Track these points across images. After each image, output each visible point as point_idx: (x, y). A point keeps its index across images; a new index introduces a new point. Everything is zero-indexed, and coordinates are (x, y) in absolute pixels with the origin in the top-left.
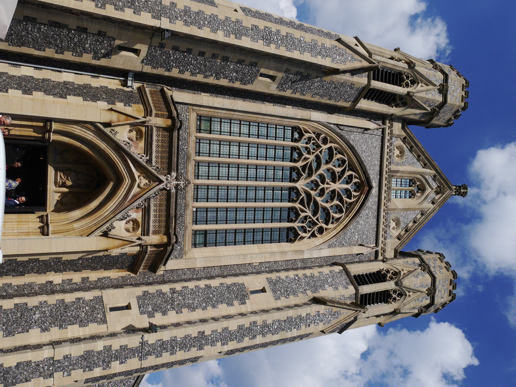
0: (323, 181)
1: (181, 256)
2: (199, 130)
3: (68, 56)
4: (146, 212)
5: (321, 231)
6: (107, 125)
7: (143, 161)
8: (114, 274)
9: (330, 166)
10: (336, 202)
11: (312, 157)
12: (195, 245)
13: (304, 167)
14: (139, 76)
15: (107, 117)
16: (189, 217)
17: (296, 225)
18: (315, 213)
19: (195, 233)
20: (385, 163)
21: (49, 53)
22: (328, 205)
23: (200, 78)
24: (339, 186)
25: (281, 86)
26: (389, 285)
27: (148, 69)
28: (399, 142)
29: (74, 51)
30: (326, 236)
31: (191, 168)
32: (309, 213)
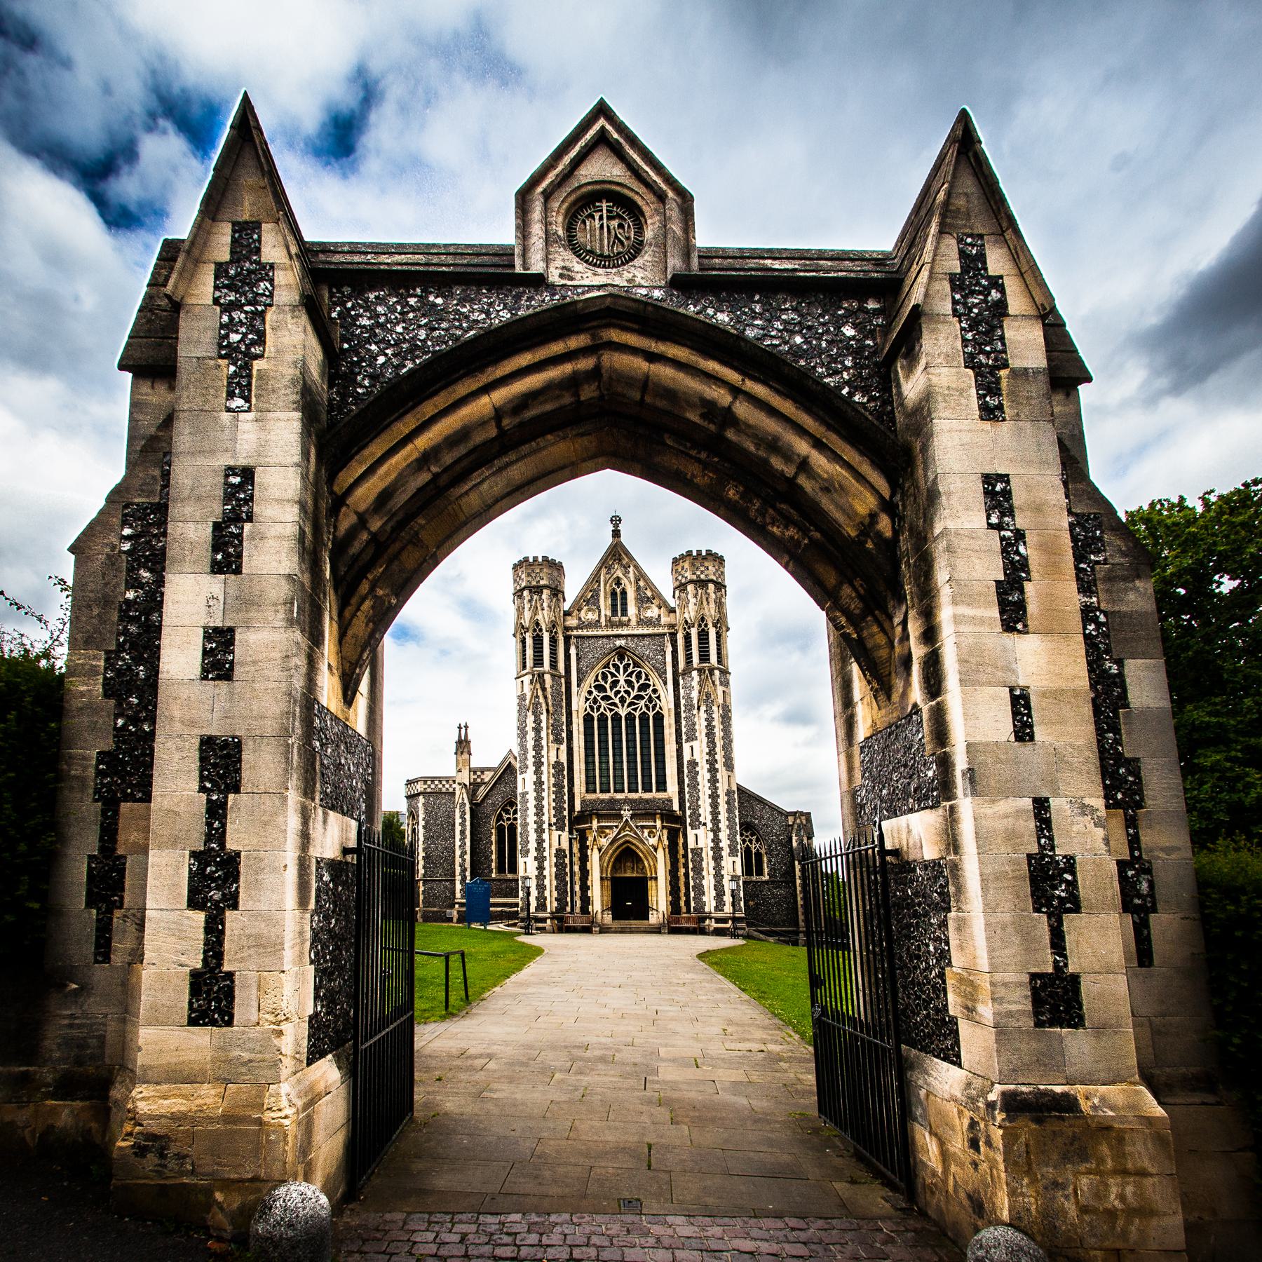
0: (619, 692)
1: (670, 801)
2: (595, 791)
3: (568, 870)
4: (643, 827)
5: (655, 691)
6: (600, 850)
7: (616, 831)
8: (681, 841)
9: (608, 686)
10: (633, 679)
11: (603, 704)
12: (665, 790)
13: (611, 710)
14: (571, 832)
15: (596, 851)
16: (647, 796)
17: (651, 714)
18: (642, 698)
19: (658, 790)
20: (600, 633)
21: (568, 879)
22: (636, 686)
23: (566, 798)
24: (622, 678)
25: (561, 743)
26: (694, 632)
27: (567, 829)
28: (583, 614)
29: (565, 867)
30: (658, 687)
31: (619, 796)
32: (642, 703)
